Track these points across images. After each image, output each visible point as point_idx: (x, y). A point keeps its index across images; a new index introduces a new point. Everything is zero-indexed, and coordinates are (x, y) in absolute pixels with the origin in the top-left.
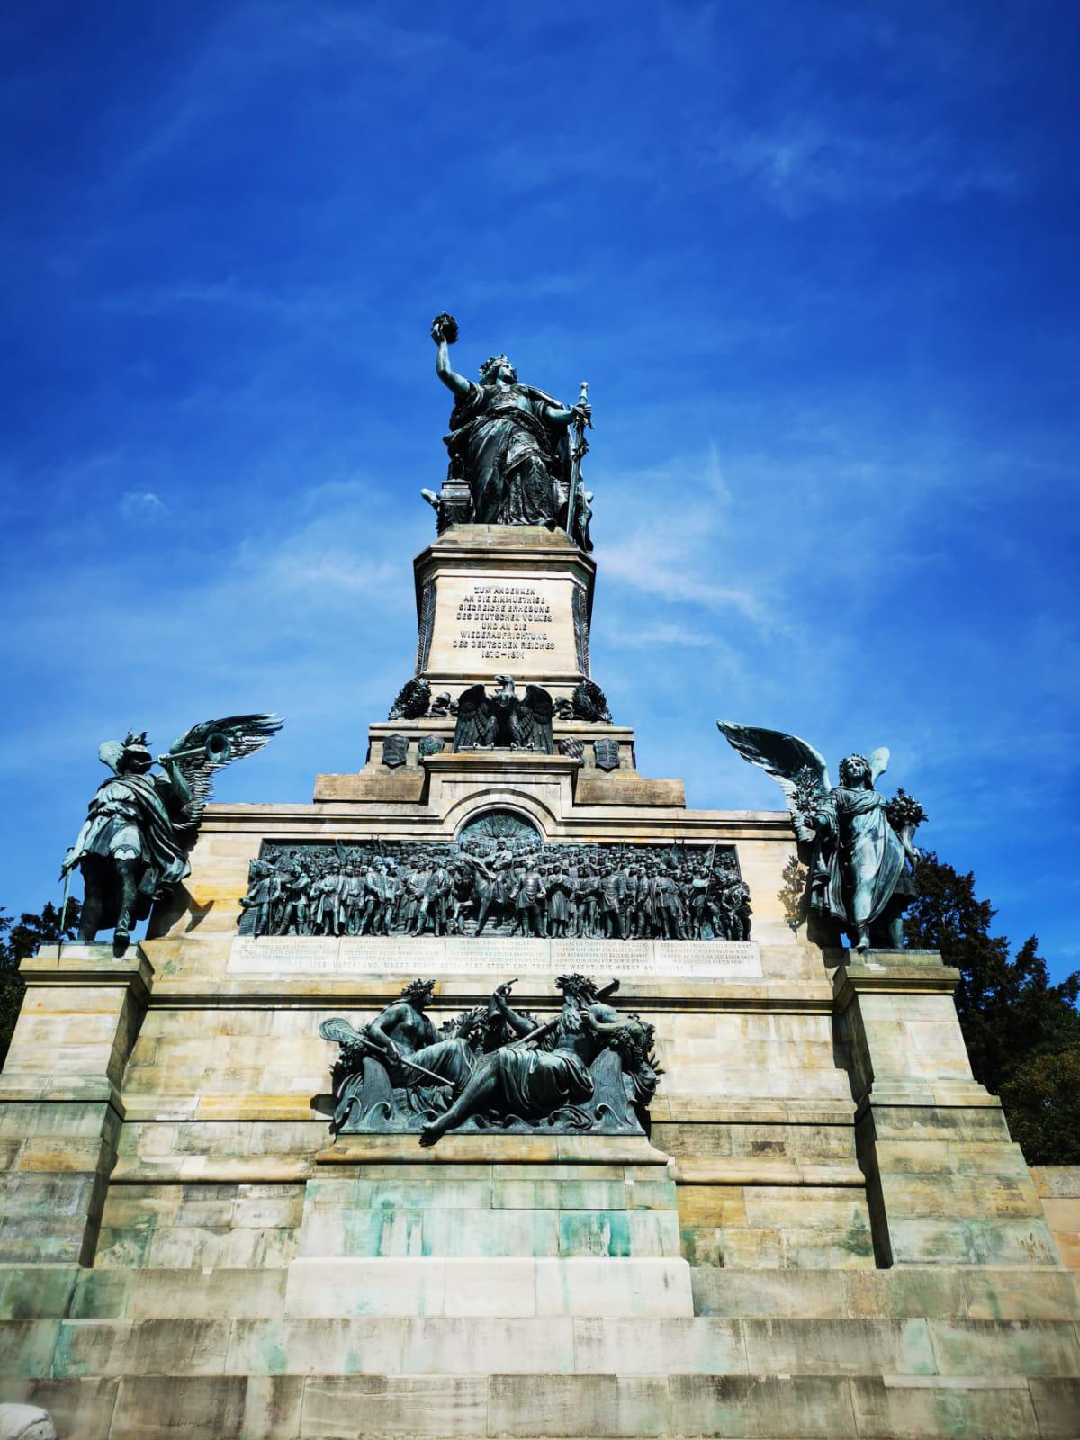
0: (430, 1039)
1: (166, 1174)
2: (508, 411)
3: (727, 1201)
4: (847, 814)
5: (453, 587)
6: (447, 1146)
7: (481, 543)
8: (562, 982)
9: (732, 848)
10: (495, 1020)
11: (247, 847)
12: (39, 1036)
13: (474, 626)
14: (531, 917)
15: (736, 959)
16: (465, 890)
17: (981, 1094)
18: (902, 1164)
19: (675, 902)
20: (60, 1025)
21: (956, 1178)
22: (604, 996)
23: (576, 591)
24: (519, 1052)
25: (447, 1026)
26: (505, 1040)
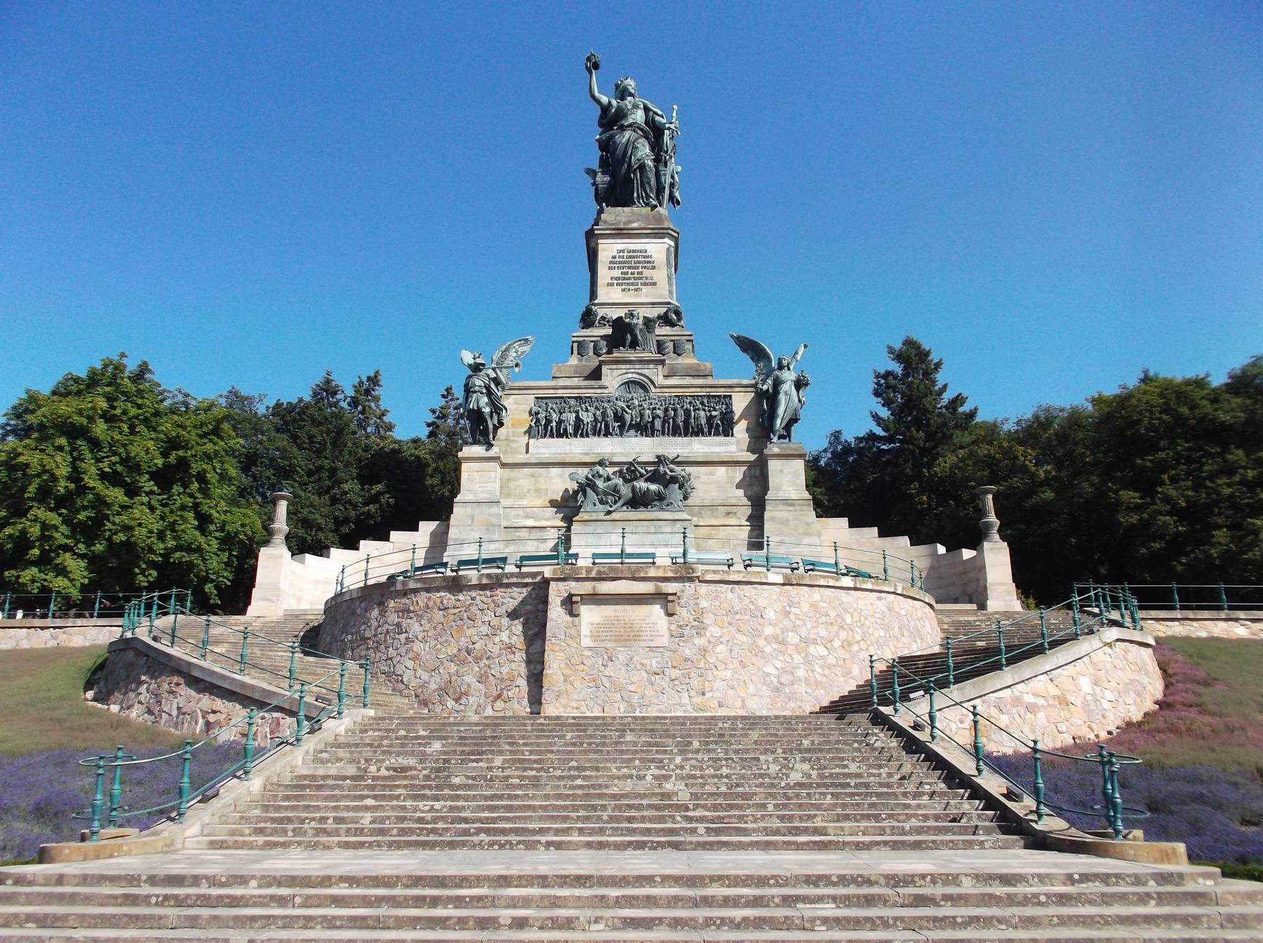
0: (608, 479)
1: (521, 524)
2: (630, 126)
3: (713, 532)
4: (777, 383)
5: (608, 249)
6: (614, 516)
7: (619, 222)
8: (658, 457)
9: (730, 397)
10: (630, 471)
11: (529, 401)
12: (470, 480)
13: (617, 273)
14: (644, 429)
15: (727, 444)
16: (619, 418)
17: (807, 495)
18: (772, 519)
19: (703, 421)
20: (477, 476)
21: (791, 523)
22: (673, 462)
23: (668, 250)
24: (642, 485)
25: (614, 473)
26: (636, 479)
